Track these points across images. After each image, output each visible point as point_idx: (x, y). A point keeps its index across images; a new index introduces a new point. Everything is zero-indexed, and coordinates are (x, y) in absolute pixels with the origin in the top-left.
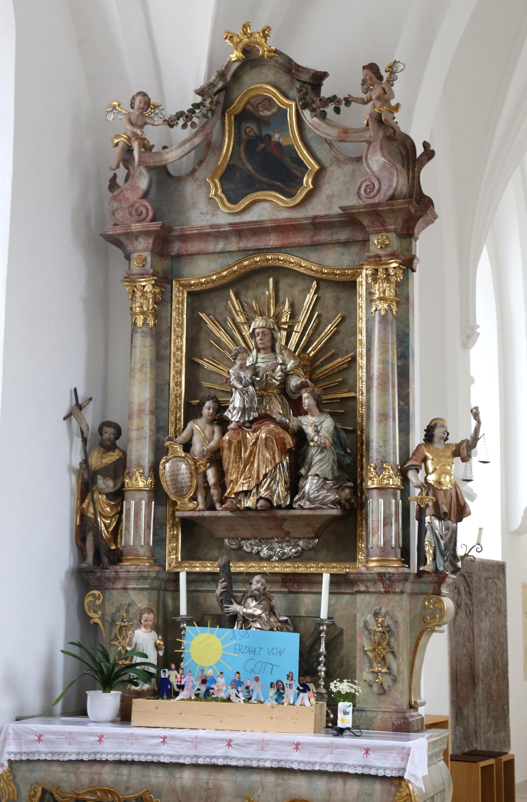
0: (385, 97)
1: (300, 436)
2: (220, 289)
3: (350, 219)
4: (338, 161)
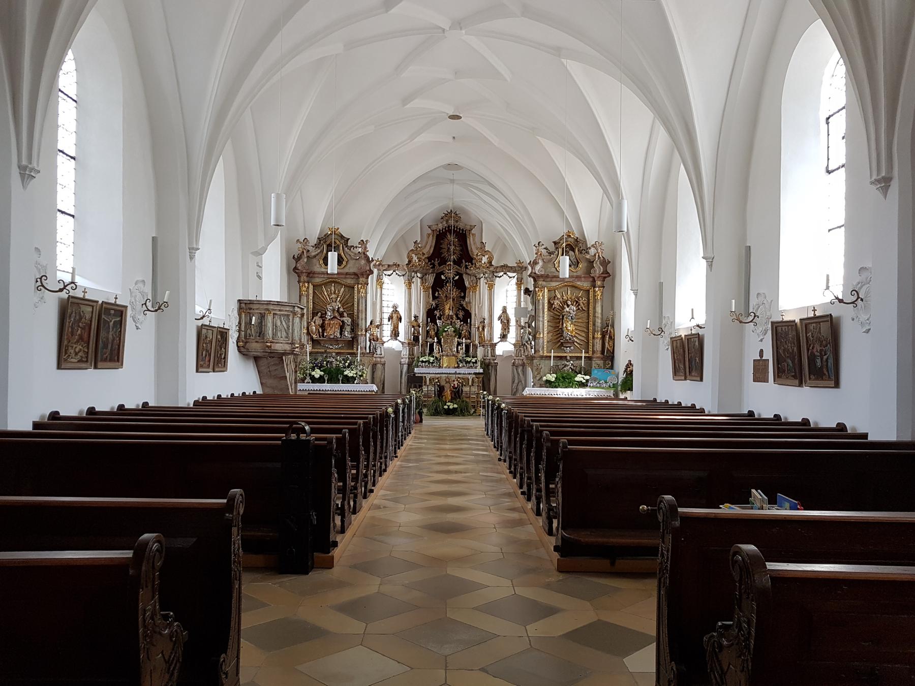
0: (366, 248)
1: (343, 322)
2: (321, 285)
3: (355, 274)
4: (352, 259)
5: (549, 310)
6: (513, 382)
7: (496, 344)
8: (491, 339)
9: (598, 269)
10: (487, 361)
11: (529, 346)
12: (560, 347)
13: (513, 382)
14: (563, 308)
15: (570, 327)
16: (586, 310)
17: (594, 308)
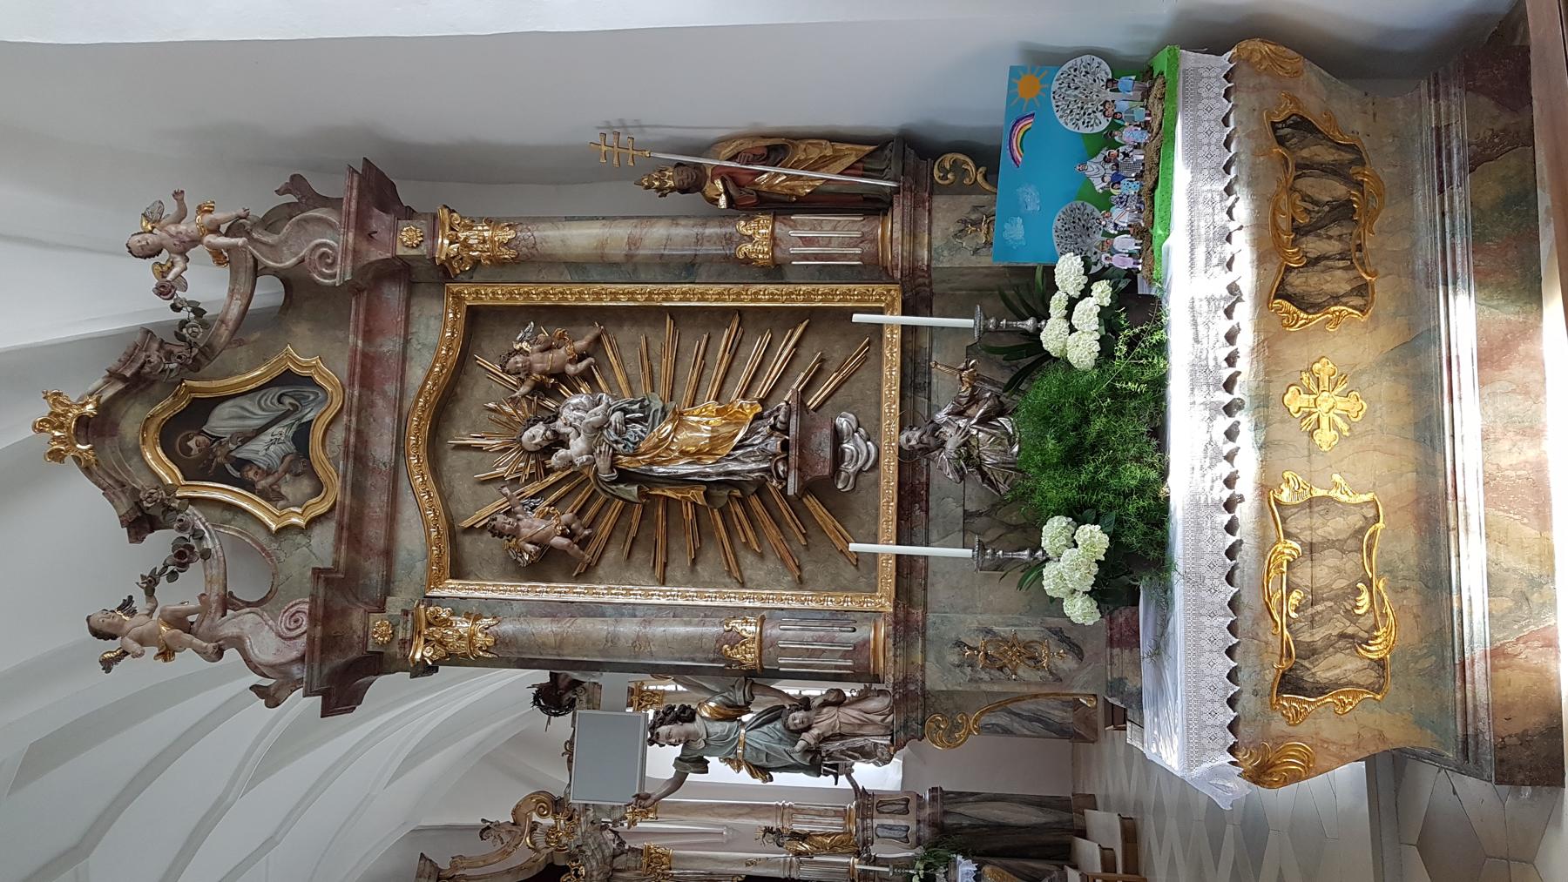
5: (585, 574)
6: (1006, 731)
7: (861, 793)
8: (844, 814)
9: (326, 245)
10: (926, 832)
11: (827, 720)
12: (839, 505)
13: (1006, 731)
14: (575, 477)
15: (702, 426)
16: (588, 326)
17: (579, 267)
